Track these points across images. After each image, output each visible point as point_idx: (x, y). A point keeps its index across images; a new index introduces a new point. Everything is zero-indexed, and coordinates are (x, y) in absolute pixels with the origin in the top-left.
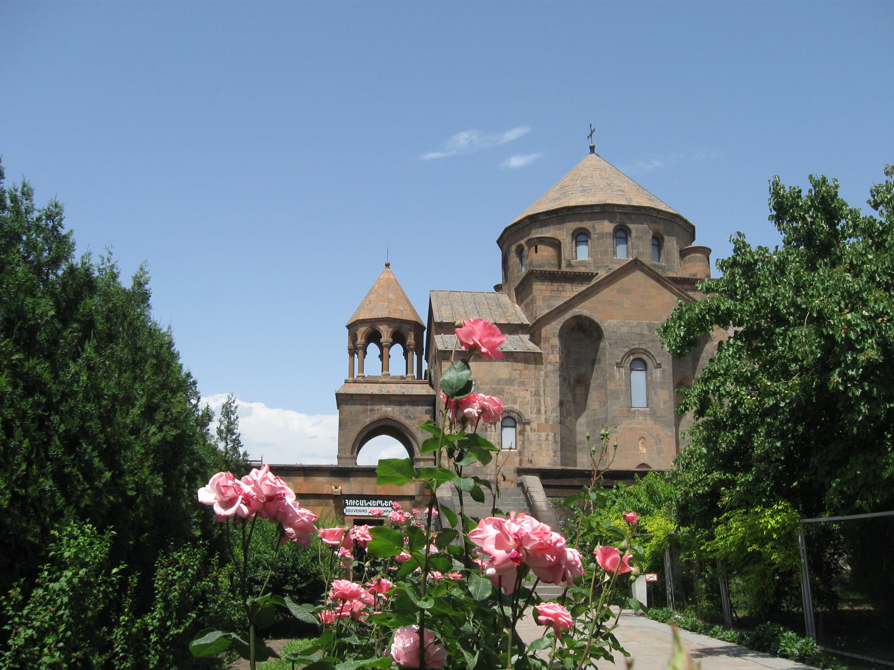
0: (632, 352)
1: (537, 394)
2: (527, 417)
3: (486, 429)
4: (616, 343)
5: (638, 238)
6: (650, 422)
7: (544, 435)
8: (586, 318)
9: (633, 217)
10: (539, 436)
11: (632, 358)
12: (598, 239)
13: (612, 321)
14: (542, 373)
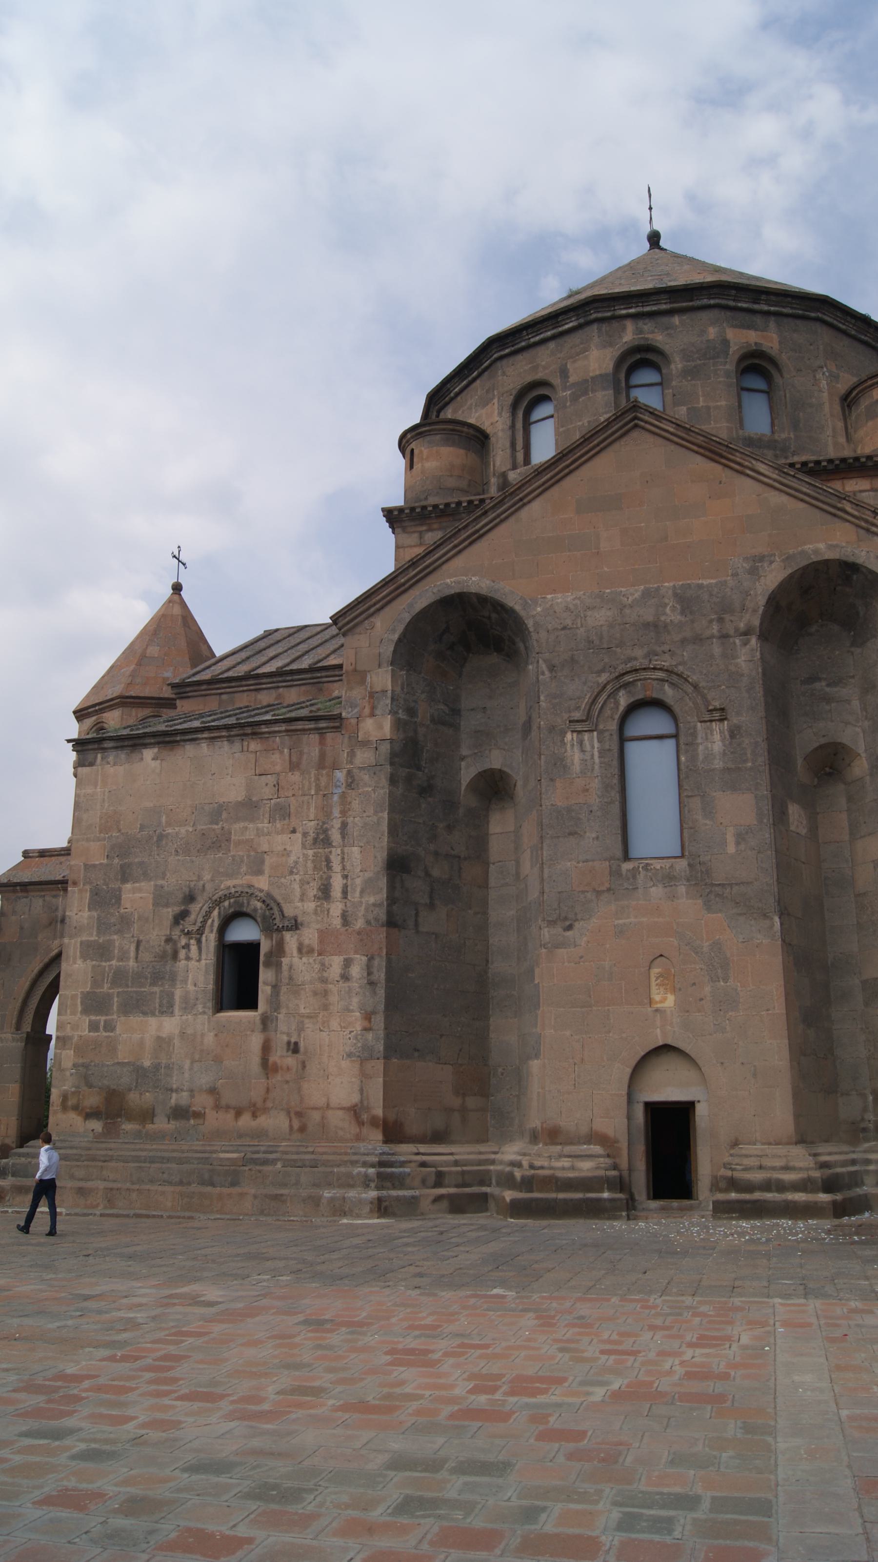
0: (621, 681)
1: (322, 839)
2: (289, 911)
3: (175, 956)
4: (573, 660)
5: (690, 373)
6: (687, 906)
7: (336, 963)
8: (483, 600)
9: (676, 320)
10: (324, 967)
11: (624, 700)
12: (575, 398)
13: (560, 599)
14: (340, 775)
